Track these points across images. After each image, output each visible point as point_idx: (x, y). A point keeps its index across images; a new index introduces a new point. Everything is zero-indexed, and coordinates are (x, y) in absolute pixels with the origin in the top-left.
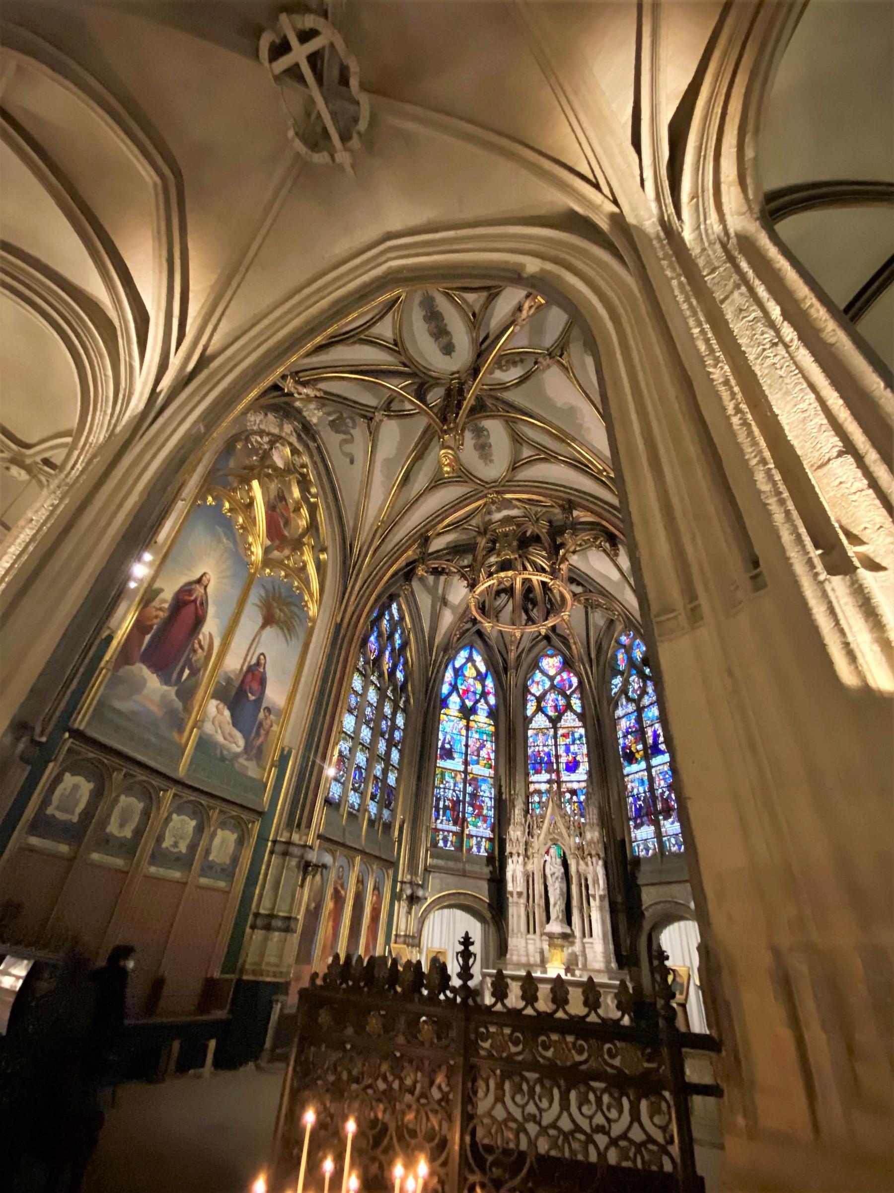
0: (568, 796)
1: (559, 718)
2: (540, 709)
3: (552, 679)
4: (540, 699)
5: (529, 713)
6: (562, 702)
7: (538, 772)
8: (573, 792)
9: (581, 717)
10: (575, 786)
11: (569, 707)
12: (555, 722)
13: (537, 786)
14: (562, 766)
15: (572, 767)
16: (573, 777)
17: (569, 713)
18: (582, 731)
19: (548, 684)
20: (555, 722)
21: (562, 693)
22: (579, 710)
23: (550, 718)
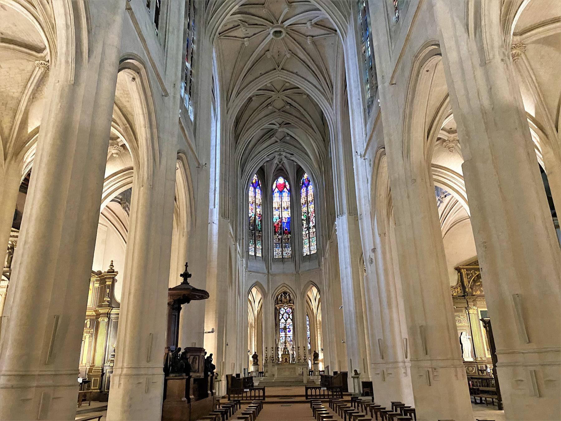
0: (288, 337)
1: (287, 320)
2: (282, 317)
3: (286, 310)
4: (283, 315)
5: (280, 318)
6: (288, 316)
7: (282, 332)
8: (289, 337)
9: (292, 320)
10: (290, 335)
11: (289, 317)
12: (286, 321)
13: (282, 336)
14: (287, 331)
15: (289, 332)
16: (289, 333)
17: (289, 319)
18: (292, 323)
19: (284, 312)
20: (286, 321)
21: (288, 313)
22: (291, 318)
23: (285, 320)
